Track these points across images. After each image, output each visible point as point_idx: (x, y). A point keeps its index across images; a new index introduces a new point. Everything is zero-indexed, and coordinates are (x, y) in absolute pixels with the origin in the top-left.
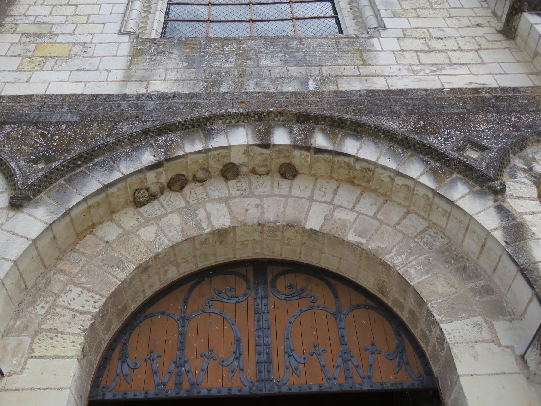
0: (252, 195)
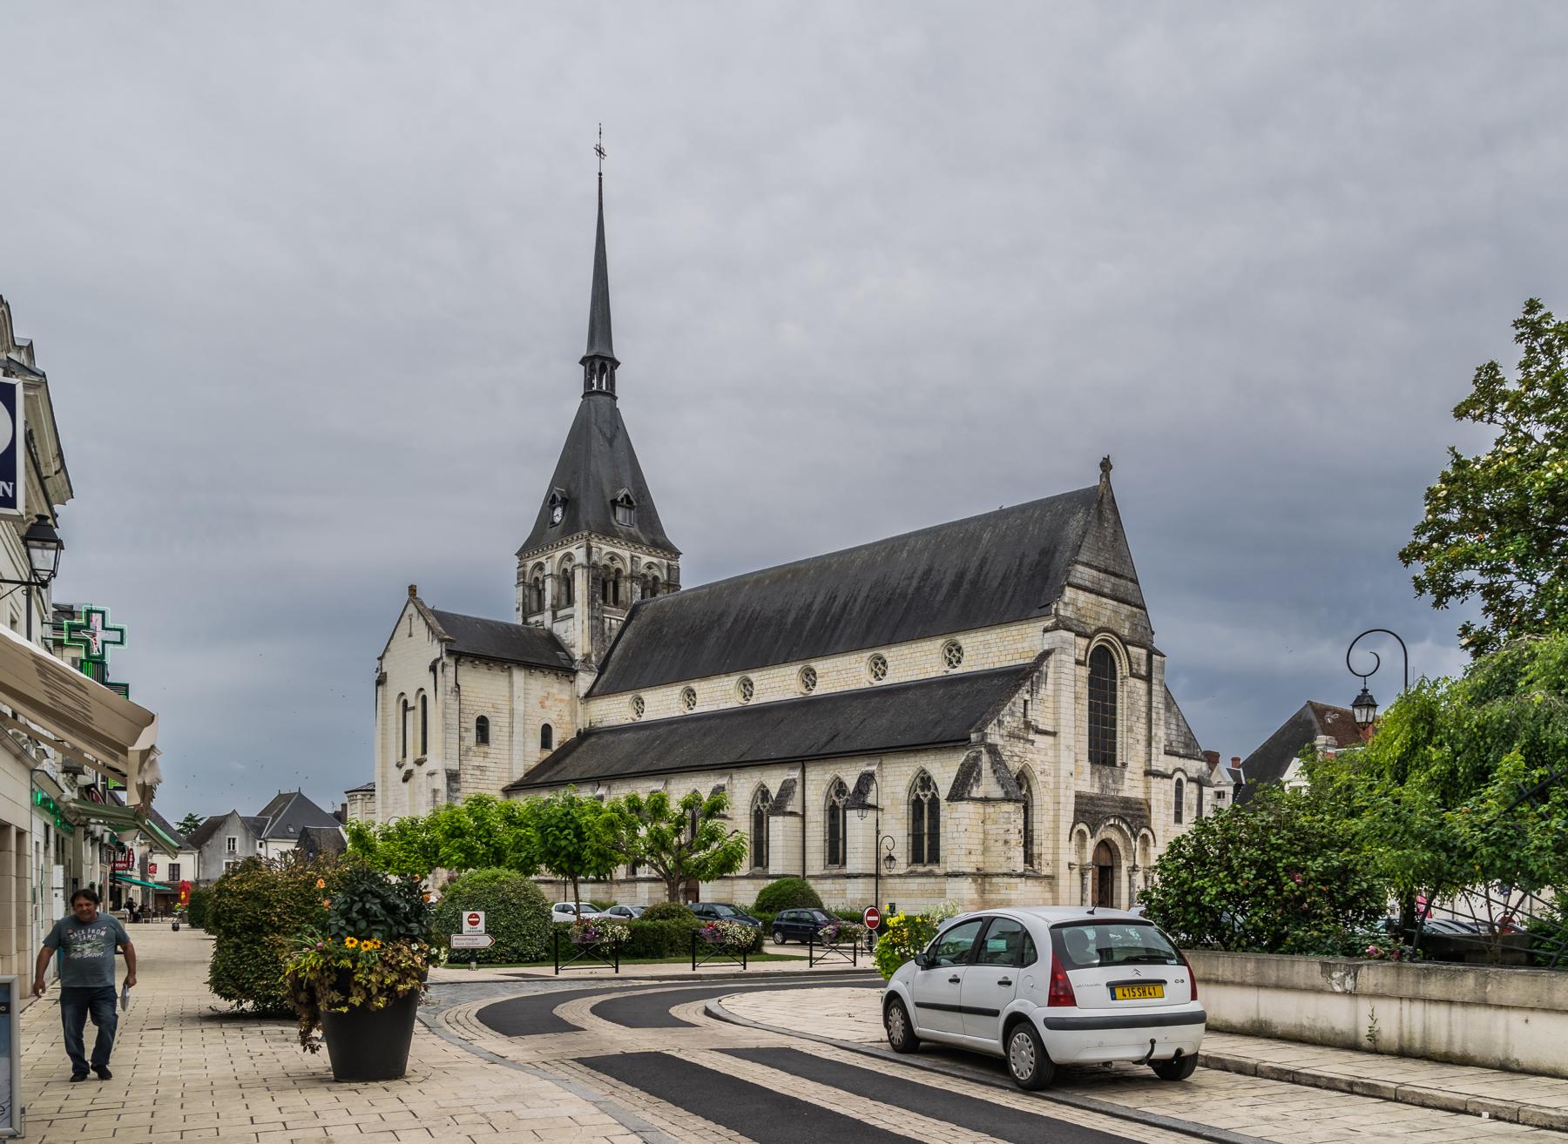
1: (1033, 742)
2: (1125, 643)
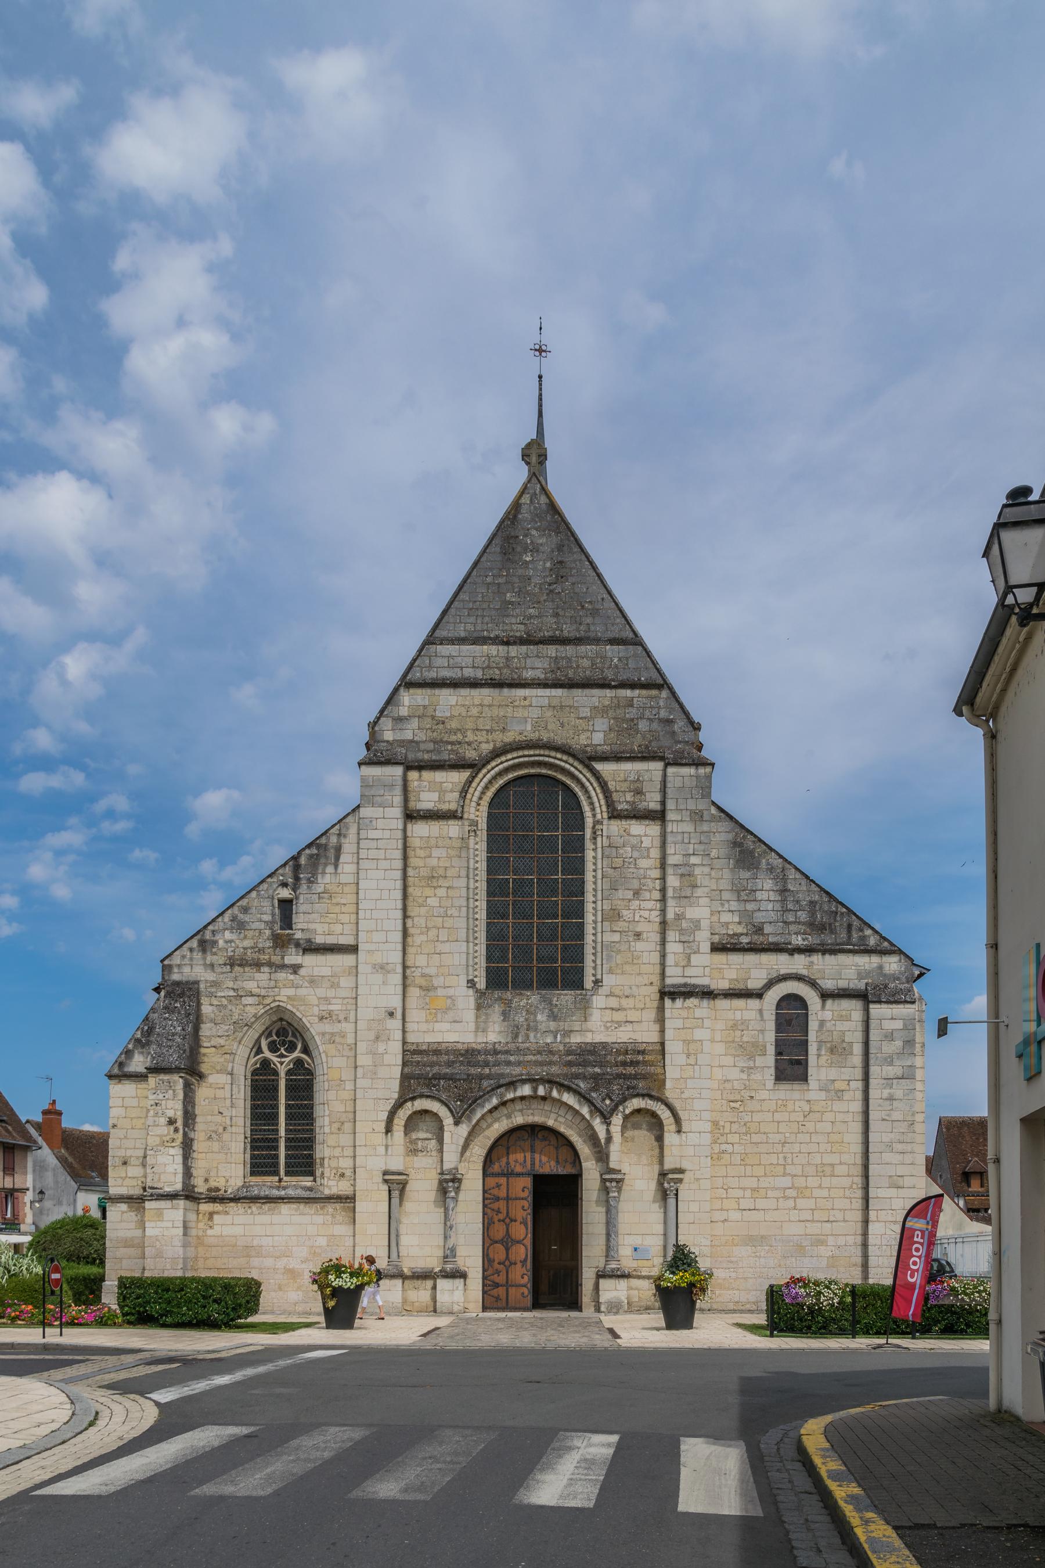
1: (295, 969)
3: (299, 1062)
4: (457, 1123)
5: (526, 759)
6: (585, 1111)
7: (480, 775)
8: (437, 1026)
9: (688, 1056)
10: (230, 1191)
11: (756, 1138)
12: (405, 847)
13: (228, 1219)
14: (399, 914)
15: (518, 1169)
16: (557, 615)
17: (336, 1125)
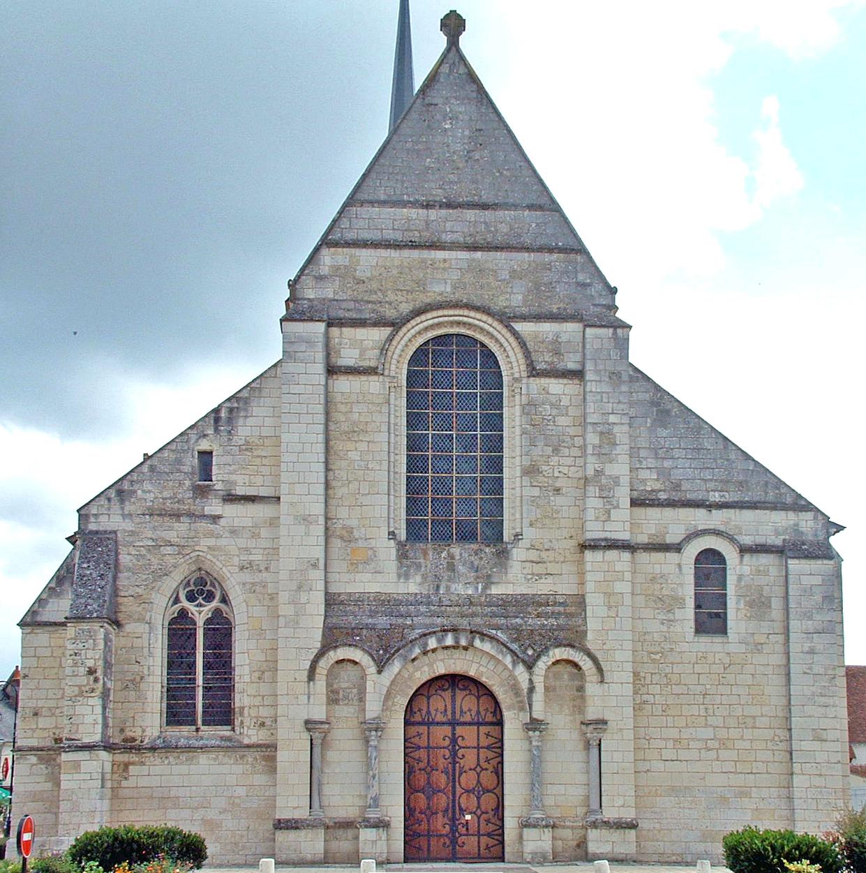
0: (451, 659)
1: (215, 519)
2: (506, 319)
3: (217, 612)
4: (379, 672)
5: (446, 319)
6: (508, 660)
7: (401, 333)
8: (358, 577)
9: (610, 607)
10: (146, 741)
11: (676, 690)
12: (327, 402)
13: (145, 770)
14: (321, 467)
15: (440, 718)
16: (475, 182)
17: (257, 674)
